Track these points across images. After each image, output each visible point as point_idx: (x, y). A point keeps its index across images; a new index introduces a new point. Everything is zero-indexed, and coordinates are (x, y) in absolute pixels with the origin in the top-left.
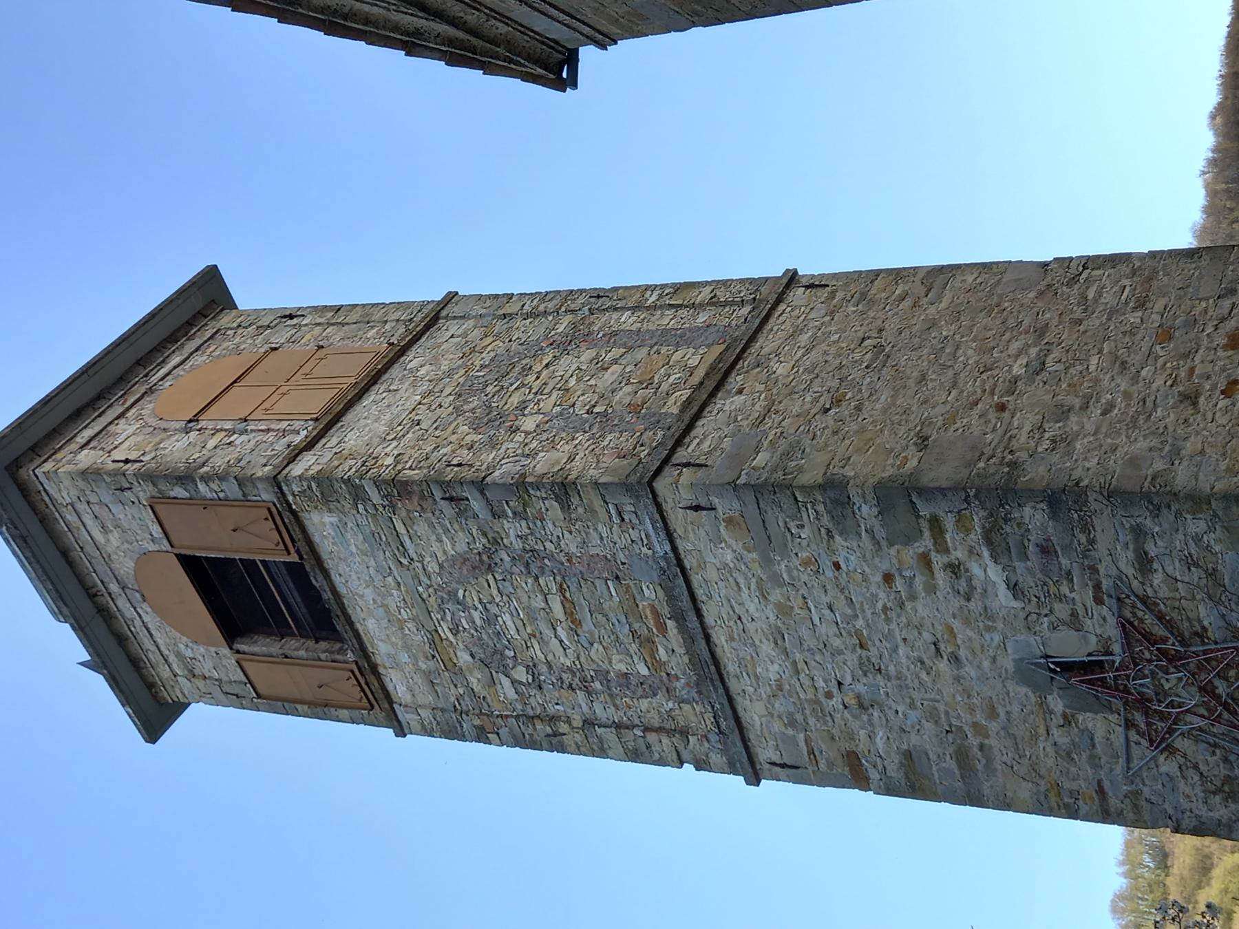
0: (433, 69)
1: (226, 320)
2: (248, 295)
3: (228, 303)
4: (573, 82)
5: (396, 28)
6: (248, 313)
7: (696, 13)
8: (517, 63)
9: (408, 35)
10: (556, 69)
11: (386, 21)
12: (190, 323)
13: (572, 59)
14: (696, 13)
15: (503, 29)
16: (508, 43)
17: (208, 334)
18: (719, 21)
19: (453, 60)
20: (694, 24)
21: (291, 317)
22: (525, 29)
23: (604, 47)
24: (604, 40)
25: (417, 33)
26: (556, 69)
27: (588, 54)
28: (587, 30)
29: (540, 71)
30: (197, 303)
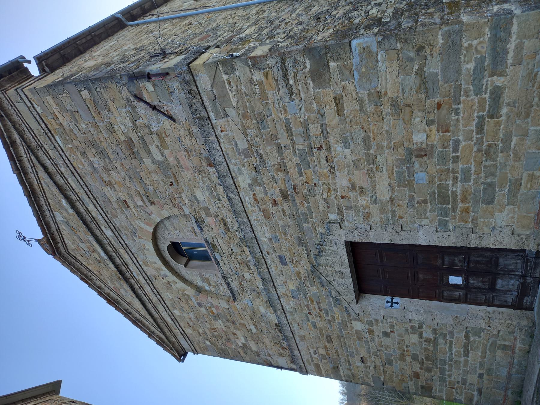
0: (152, 343)
1: (54, 397)
2: (64, 392)
3: (58, 392)
4: (183, 361)
5: (149, 329)
6: (61, 397)
7: (220, 353)
8: (173, 350)
9: (151, 332)
10: (181, 355)
11: (148, 327)
12: (44, 395)
13: (185, 355)
14: (220, 353)
15: (174, 340)
16: (173, 344)
17: (47, 399)
18: (224, 357)
19: (158, 343)
20: (218, 356)
21: (73, 402)
22: (179, 342)
23: (194, 354)
24: (195, 352)
25: (153, 333)
26: (181, 355)
27: (190, 355)
28: (193, 348)
29: (177, 354)
30: (50, 389)
